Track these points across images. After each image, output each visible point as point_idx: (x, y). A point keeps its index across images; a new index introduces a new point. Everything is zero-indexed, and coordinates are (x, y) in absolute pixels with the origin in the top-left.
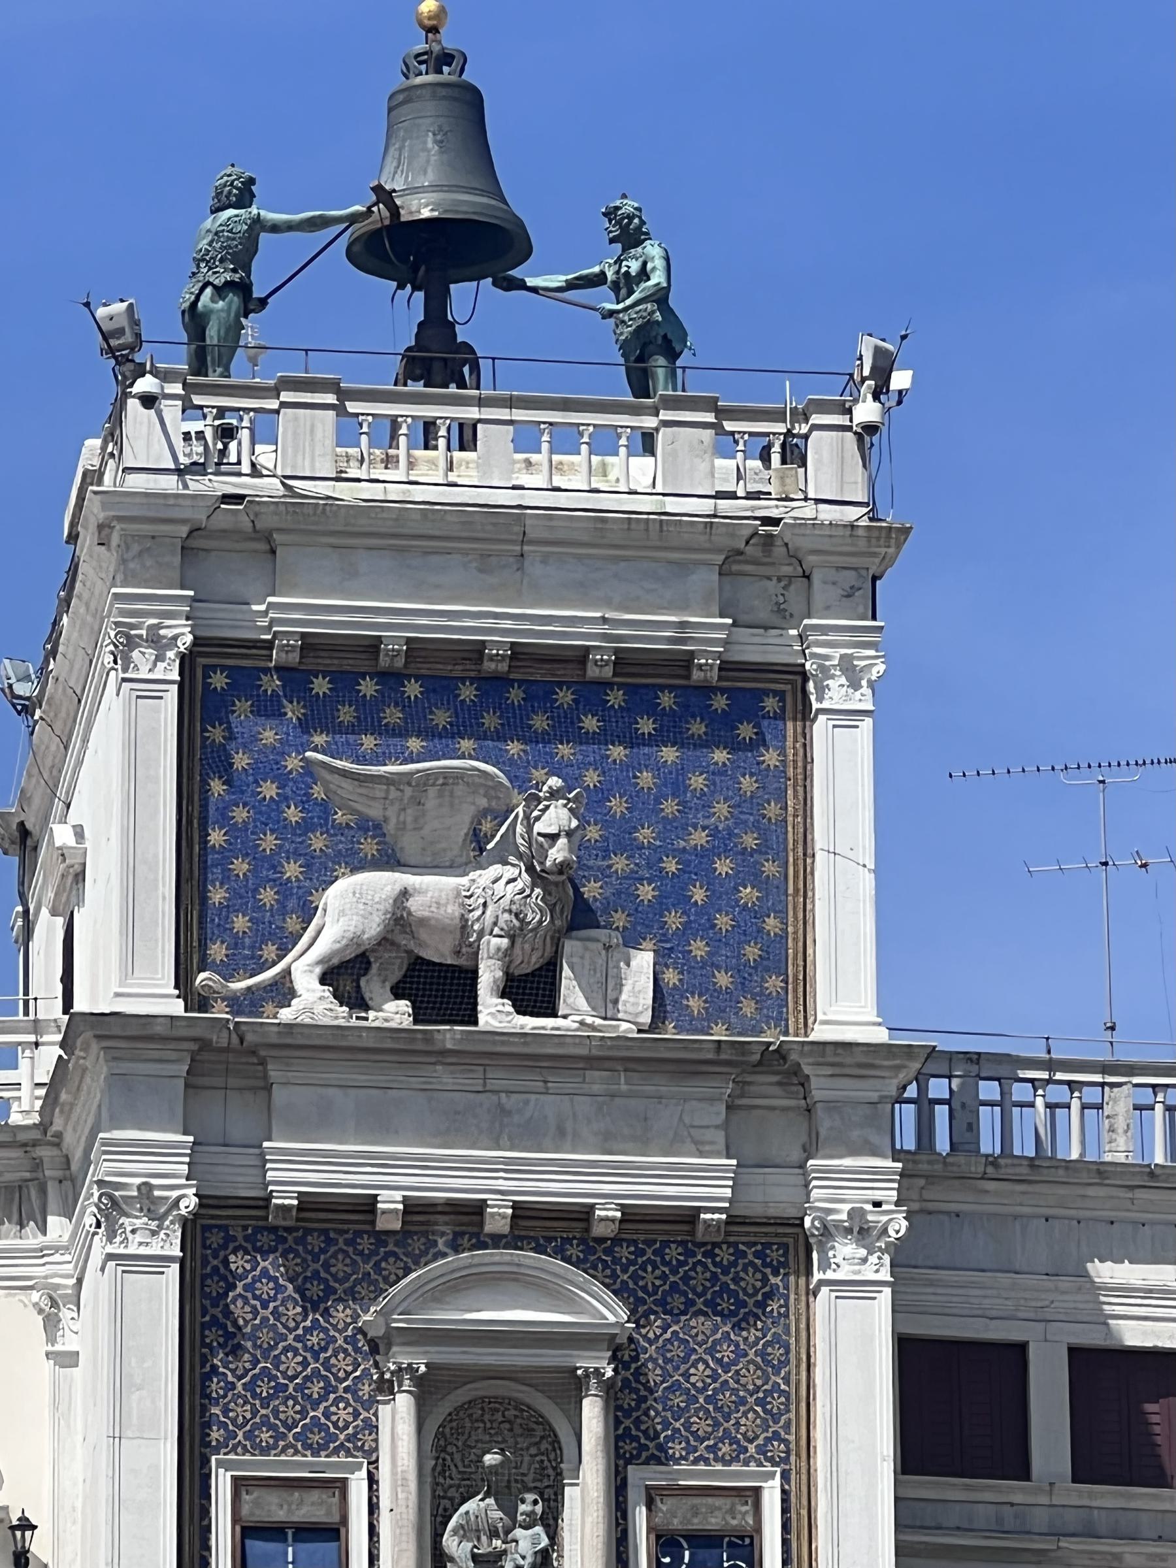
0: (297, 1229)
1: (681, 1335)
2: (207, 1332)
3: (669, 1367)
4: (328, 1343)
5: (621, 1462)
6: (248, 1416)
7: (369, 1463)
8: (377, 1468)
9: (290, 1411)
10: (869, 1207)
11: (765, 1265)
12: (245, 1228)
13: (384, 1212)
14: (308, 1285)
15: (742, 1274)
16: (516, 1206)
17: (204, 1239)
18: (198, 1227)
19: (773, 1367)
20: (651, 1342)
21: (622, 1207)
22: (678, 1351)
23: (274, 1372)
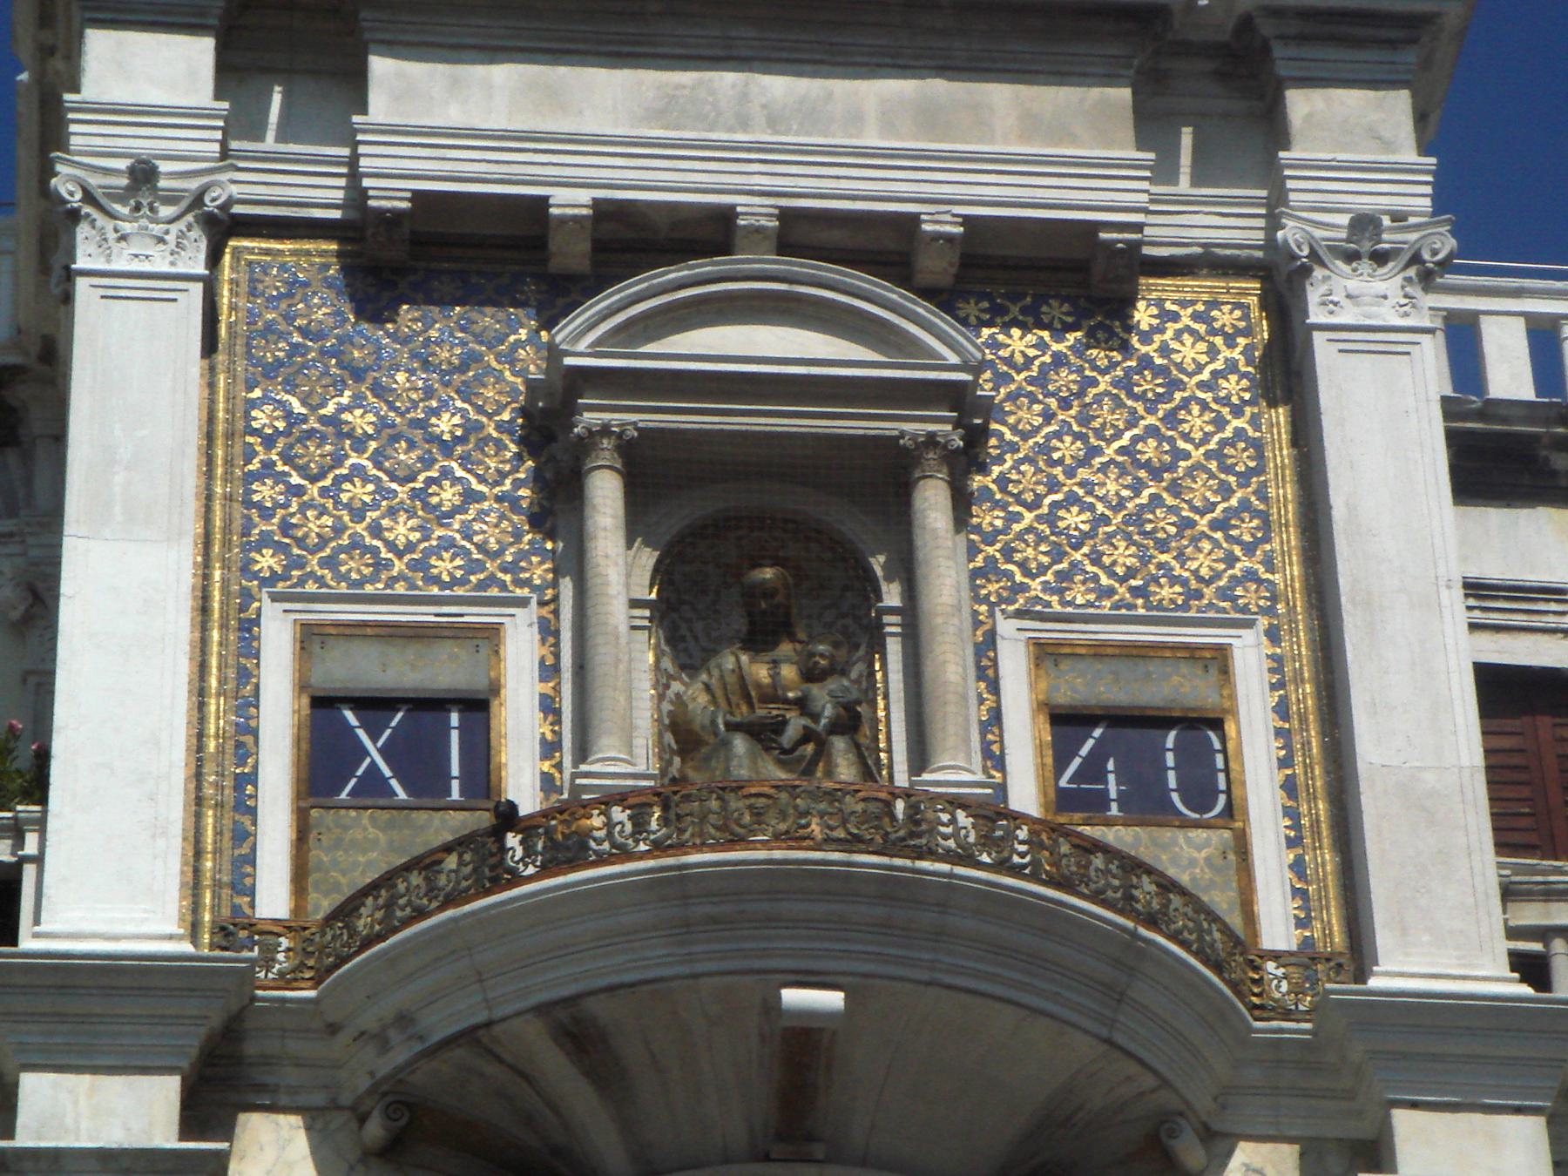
1: (1076, 428)
3: (1058, 471)
5: (984, 608)
7: (542, 604)
8: (556, 612)
9: (402, 531)
10: (1386, 221)
11: (1213, 332)
13: (563, 220)
15: (1174, 345)
16: (785, 215)
19: (1238, 474)
20: (1025, 436)
21: (967, 220)
22: (1068, 448)
23: (375, 472)
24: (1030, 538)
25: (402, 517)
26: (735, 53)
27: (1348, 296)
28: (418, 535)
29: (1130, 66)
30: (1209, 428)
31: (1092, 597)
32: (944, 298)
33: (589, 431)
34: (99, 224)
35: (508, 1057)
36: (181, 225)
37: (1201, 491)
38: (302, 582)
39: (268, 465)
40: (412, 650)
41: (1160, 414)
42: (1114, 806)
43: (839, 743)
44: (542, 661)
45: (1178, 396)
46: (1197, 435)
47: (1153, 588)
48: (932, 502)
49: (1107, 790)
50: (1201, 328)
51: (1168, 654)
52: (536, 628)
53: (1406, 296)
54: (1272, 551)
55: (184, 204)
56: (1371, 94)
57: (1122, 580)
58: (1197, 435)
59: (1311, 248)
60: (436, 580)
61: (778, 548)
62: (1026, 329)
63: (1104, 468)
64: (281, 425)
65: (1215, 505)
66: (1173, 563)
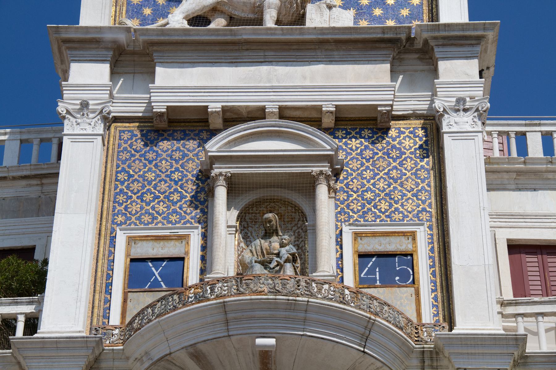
0: (170, 130)
2: (119, 175)
4: (183, 177)
5: (339, 224)
6: (139, 210)
9: (161, 208)
11: (415, 136)
12: (143, 131)
13: (212, 113)
14: (174, 153)
15: (403, 141)
16: (281, 108)
17: (120, 136)
18: (118, 131)
19: (421, 179)
21: (337, 106)
22: (368, 174)
24: (355, 202)
25: (162, 204)
26: (267, 60)
27: (456, 123)
28: (166, 209)
29: (389, 57)
30: (413, 166)
31: (374, 219)
32: (330, 132)
33: (216, 175)
34: (71, 120)
35: (177, 364)
36: (96, 119)
37: (409, 185)
38: (130, 224)
39: (121, 190)
40: (162, 243)
41: (398, 162)
42: (378, 282)
43: (288, 266)
44: (202, 245)
45: (404, 156)
46: (409, 168)
47: (393, 215)
48: (322, 191)
49: (376, 277)
50: (412, 135)
51: (396, 235)
52: (200, 235)
53: (474, 122)
54: (431, 202)
55: (97, 113)
56: (465, 61)
57: (383, 213)
58: (409, 168)
59: (444, 109)
60: (171, 222)
61: (276, 207)
62: (356, 138)
63: (379, 180)
64: (126, 178)
65: (413, 189)
66: (400, 207)
